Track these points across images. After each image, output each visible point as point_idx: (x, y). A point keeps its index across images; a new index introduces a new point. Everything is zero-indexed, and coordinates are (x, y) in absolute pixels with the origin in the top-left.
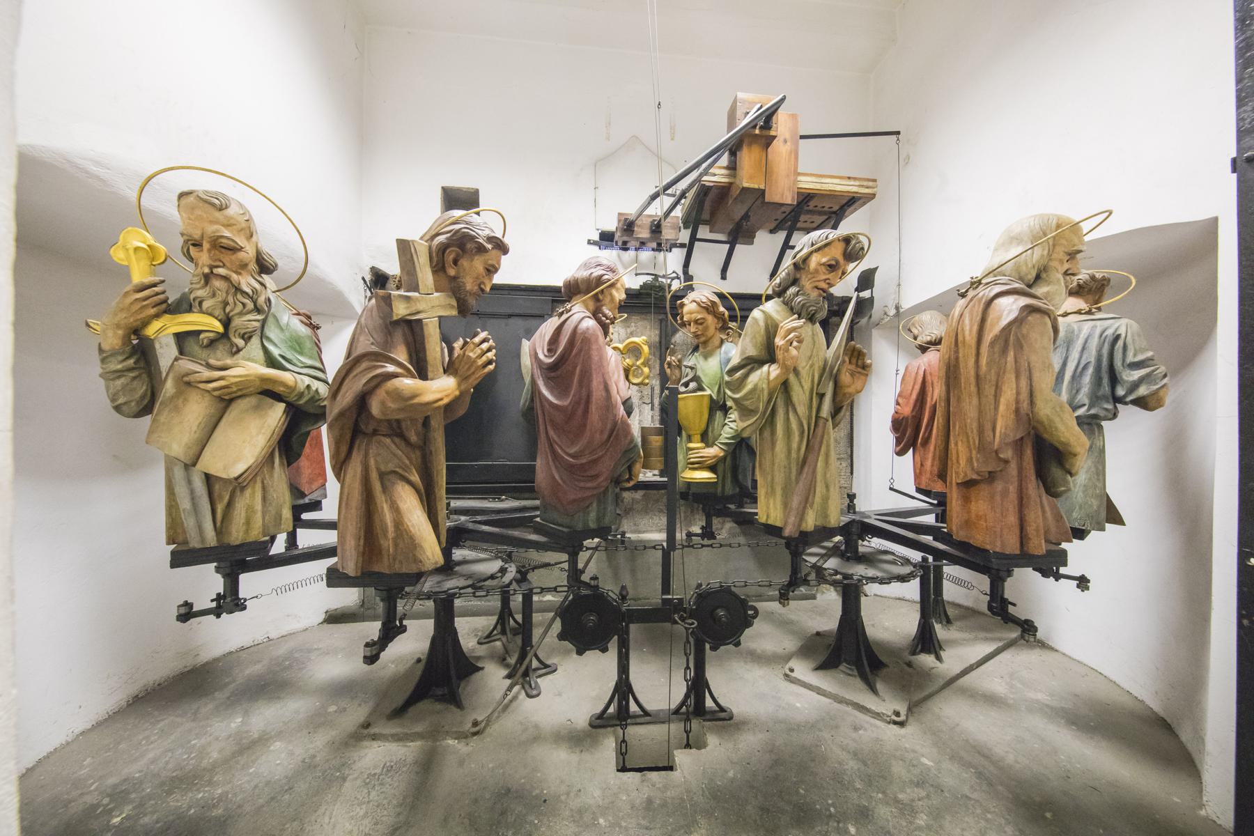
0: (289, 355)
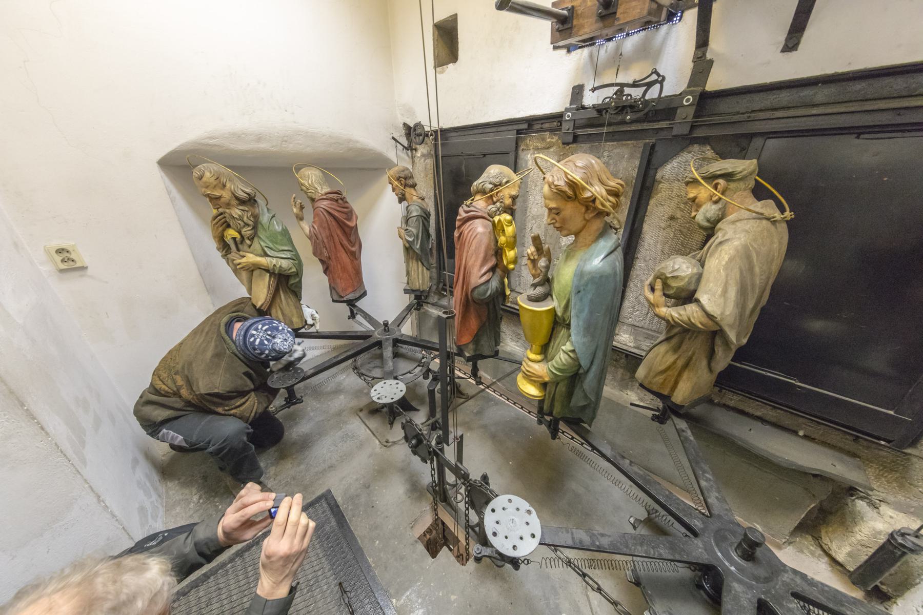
0: (271, 245)
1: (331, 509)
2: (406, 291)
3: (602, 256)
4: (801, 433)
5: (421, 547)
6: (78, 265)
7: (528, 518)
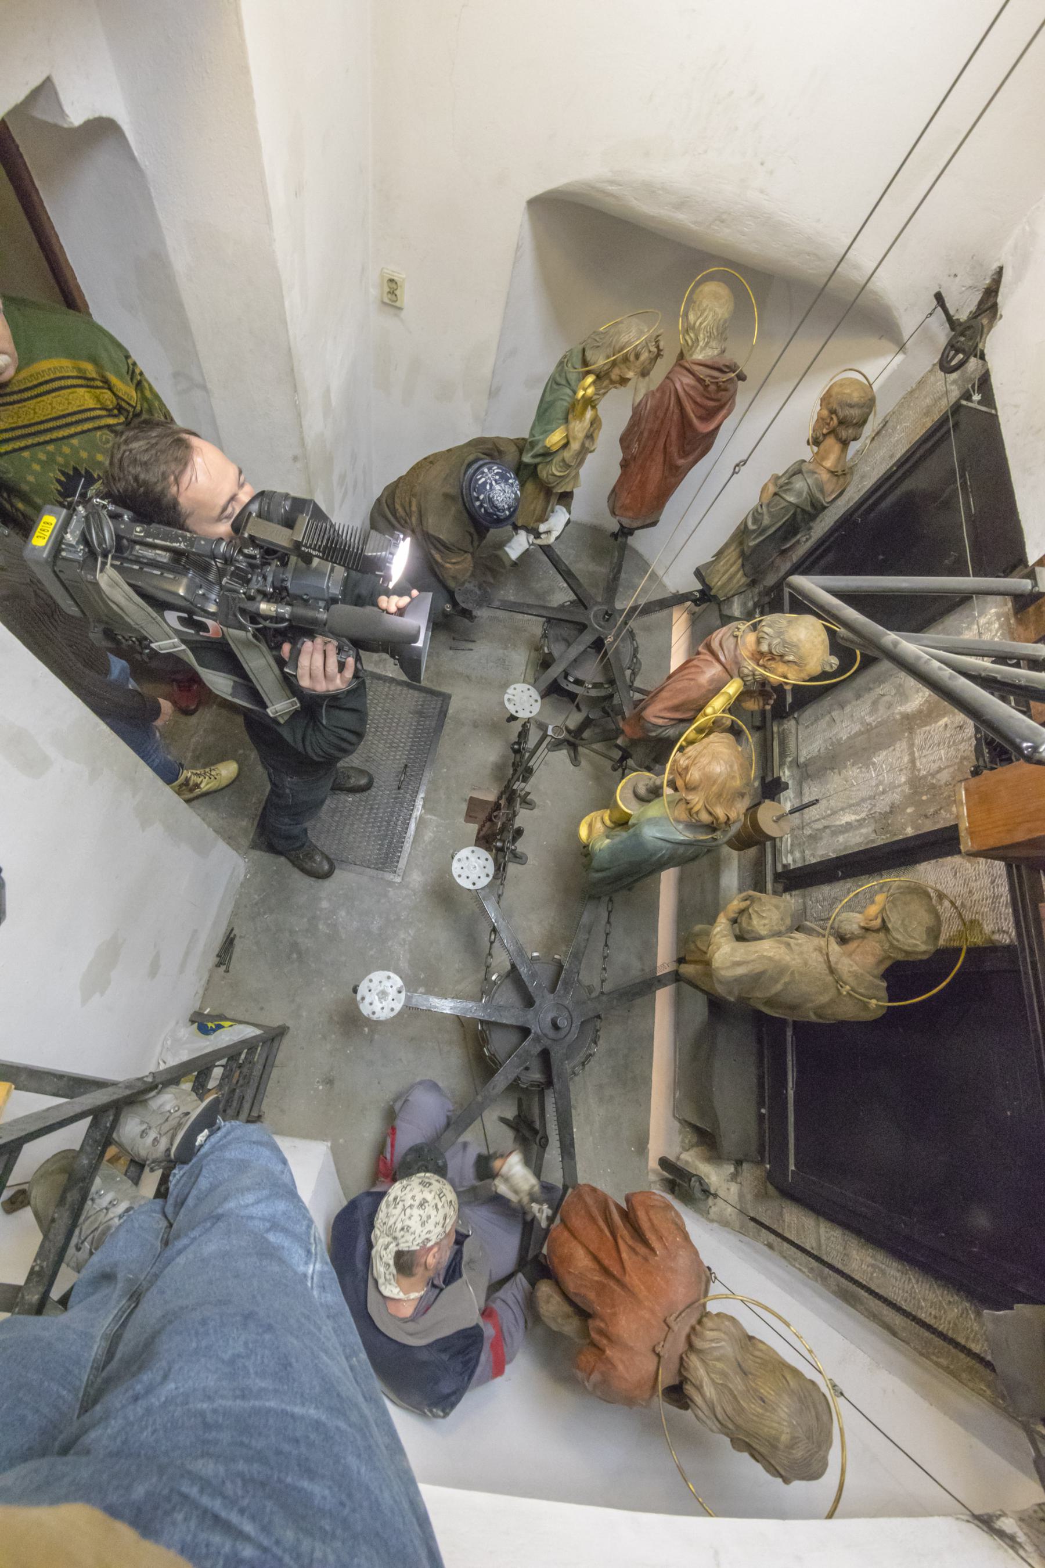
1: (440, 712)
2: (698, 573)
3: (658, 835)
4: (763, 1111)
5: (464, 806)
6: (398, 304)
7: (483, 876)
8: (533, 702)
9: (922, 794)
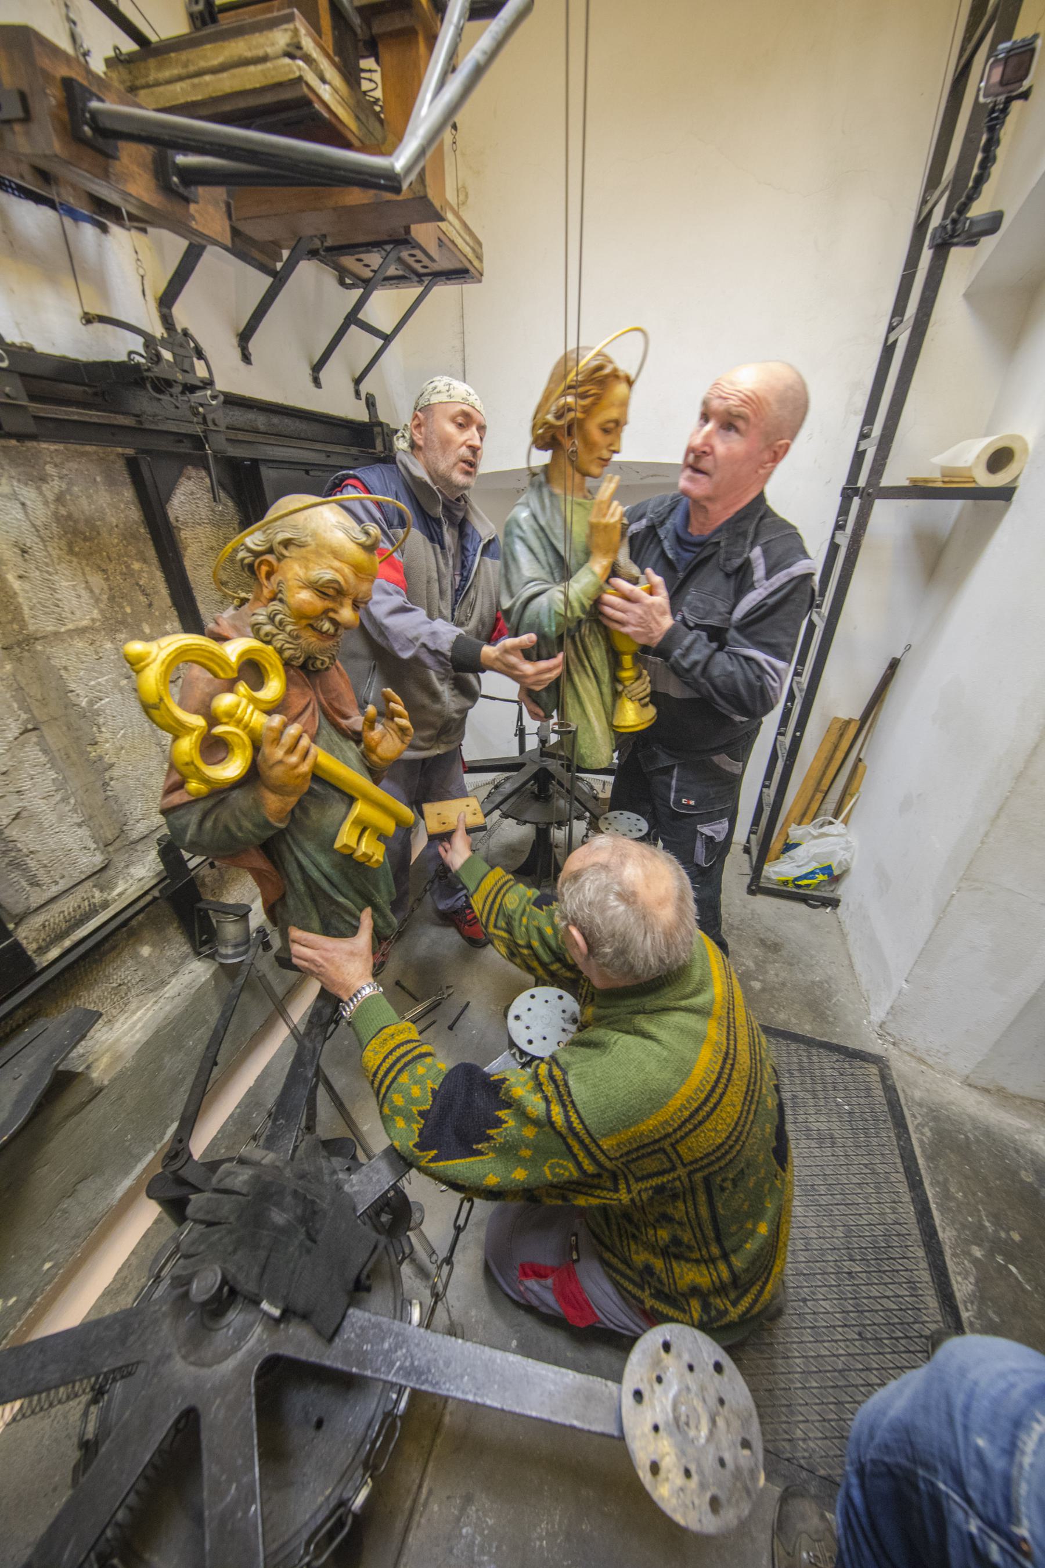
8: (524, 1017)
9: (124, 614)
